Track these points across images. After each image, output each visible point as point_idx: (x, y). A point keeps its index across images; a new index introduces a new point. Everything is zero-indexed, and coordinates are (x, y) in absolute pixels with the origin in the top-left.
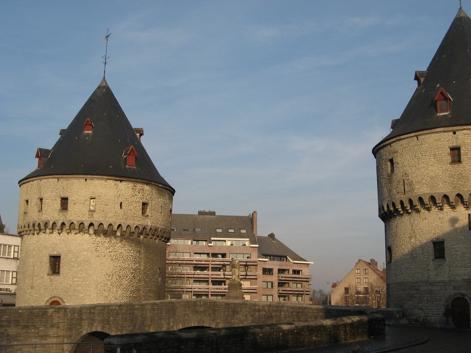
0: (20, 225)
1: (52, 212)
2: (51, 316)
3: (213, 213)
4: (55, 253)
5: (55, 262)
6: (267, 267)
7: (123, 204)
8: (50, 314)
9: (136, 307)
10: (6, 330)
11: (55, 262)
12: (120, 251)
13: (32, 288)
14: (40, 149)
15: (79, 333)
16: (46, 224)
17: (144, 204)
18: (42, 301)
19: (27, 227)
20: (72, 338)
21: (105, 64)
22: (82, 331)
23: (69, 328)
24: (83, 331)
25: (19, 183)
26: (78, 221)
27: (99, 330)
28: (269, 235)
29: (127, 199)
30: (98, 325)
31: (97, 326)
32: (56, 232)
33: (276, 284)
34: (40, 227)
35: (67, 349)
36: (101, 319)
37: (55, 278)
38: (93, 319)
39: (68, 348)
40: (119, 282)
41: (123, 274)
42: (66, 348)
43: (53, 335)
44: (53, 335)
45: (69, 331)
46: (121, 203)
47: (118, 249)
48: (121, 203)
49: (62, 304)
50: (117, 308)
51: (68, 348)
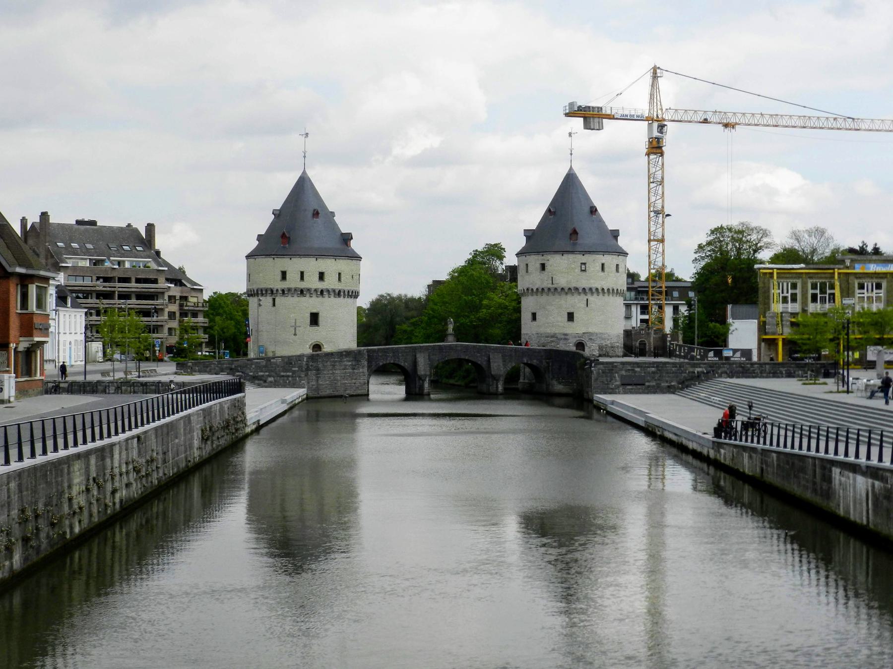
1: (312, 282)
3: (93, 223)
4: (314, 311)
6: (171, 294)
13: (295, 335)
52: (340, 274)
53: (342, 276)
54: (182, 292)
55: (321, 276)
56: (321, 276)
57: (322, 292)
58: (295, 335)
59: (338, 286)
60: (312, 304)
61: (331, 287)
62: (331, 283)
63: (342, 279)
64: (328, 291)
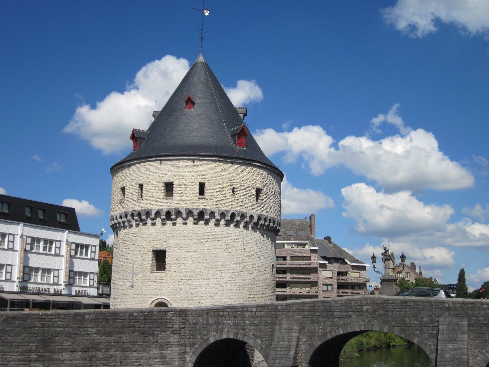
0: (116, 216)
1: (155, 200)
2: (171, 319)
4: (159, 247)
5: (160, 258)
7: (235, 190)
8: (171, 318)
9: (280, 307)
10: (120, 337)
11: (160, 258)
12: (233, 243)
13: (132, 287)
14: (135, 129)
15: (205, 340)
16: (148, 214)
17: (258, 191)
18: (146, 303)
19: (124, 218)
20: (196, 346)
21: (202, 39)
22: (209, 338)
23: (192, 334)
24: (210, 338)
25: (111, 170)
26: (186, 209)
27: (231, 337)
28: (325, 238)
29: (239, 183)
30: (229, 330)
31: (228, 332)
32: (158, 221)
33: (335, 286)
34: (142, 217)
35: (190, 360)
36: (233, 323)
37: (160, 274)
38: (223, 323)
39: (191, 359)
40: (233, 280)
41: (237, 270)
42: (188, 359)
43: (174, 343)
44: (174, 343)
45: (191, 337)
46: (234, 188)
47: (231, 242)
48: (234, 188)
49: (169, 306)
50: (254, 309)
51: (191, 359)
52: (202, 186)
53: (206, 186)
54: (339, 268)
55: (169, 188)
56: (169, 188)
57: (168, 214)
58: (132, 287)
59: (197, 204)
60: (155, 235)
61: (183, 207)
62: (186, 198)
63: (207, 191)
64: (178, 213)
